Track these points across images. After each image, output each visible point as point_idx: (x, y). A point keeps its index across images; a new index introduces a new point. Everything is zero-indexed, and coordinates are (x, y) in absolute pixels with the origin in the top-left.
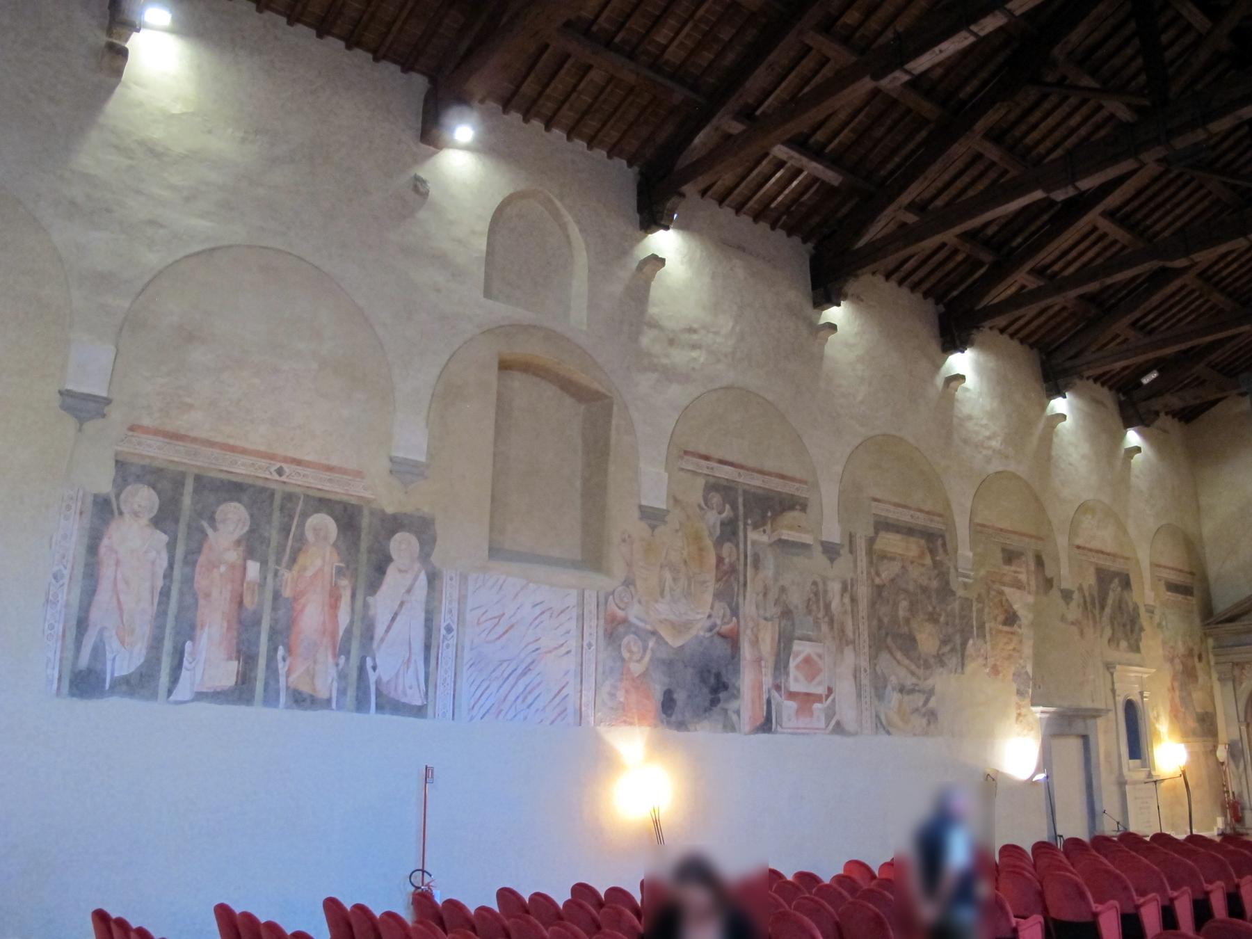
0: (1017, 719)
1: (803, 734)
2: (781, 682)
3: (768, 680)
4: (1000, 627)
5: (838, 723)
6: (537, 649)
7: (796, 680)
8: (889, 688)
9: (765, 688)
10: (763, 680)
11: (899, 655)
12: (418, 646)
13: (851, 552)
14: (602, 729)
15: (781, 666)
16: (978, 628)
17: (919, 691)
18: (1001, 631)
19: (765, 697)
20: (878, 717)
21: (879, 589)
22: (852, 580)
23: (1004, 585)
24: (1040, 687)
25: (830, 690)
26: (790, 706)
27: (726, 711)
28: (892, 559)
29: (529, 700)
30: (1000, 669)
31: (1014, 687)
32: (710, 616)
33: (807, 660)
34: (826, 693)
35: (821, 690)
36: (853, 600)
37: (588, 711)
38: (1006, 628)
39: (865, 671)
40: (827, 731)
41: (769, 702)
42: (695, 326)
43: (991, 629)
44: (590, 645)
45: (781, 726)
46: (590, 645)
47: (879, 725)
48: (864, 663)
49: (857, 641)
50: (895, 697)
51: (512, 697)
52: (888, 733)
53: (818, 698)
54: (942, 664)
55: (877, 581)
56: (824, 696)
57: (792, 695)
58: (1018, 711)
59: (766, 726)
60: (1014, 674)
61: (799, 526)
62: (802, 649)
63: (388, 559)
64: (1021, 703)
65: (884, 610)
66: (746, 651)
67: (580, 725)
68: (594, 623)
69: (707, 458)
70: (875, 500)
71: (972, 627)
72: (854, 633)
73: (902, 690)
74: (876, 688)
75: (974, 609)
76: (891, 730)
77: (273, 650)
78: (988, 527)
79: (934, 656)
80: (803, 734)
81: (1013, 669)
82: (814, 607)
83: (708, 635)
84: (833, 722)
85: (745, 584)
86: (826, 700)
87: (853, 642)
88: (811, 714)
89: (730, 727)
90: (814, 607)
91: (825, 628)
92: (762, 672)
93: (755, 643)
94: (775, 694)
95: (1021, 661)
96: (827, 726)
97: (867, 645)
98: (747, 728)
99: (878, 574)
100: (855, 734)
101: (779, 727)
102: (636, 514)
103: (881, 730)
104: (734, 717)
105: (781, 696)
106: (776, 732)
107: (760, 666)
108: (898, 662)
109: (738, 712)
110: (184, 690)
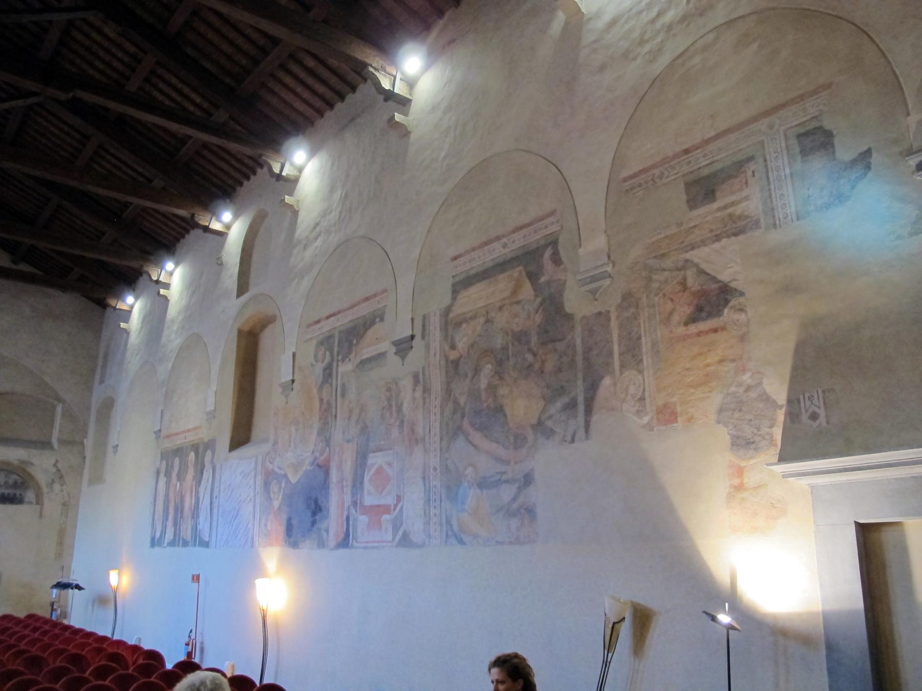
0: (730, 497)
1: (373, 548)
2: (357, 498)
3: (348, 499)
4: (681, 330)
5: (405, 535)
6: (240, 501)
7: (370, 494)
8: (466, 484)
9: (346, 505)
10: (345, 497)
11: (477, 437)
12: (209, 509)
13: (423, 337)
14: (260, 549)
15: (358, 484)
16: (621, 354)
17: (506, 481)
18: (685, 338)
19: (345, 514)
20: (448, 522)
21: (455, 365)
22: (424, 369)
23: (693, 249)
24: (814, 417)
25: (399, 498)
26: (363, 519)
27: (319, 529)
28: (474, 317)
29: (236, 534)
30: (679, 409)
31: (723, 435)
32: (313, 452)
33: (379, 471)
34: (395, 502)
35: (389, 500)
36: (426, 390)
37: (256, 538)
38: (693, 329)
39: (435, 469)
40: (394, 544)
41: (348, 519)
42: (318, 220)
43: (654, 344)
44: (258, 493)
45: (357, 542)
46: (258, 493)
47: (450, 533)
48: (434, 461)
49: (427, 437)
50: (472, 495)
51: (232, 533)
52: (461, 542)
53: (386, 509)
54: (549, 433)
55: (453, 355)
56: (392, 506)
57: (367, 510)
58: (736, 482)
59: (345, 542)
60: (720, 411)
61: (377, 339)
62: (376, 460)
63: (204, 466)
64: (743, 464)
65: (461, 389)
66: (334, 475)
67: (252, 547)
68: (260, 477)
69: (318, 322)
70: (455, 258)
71: (611, 353)
72: (424, 428)
73: (483, 484)
74: (448, 488)
75: (614, 324)
76: (464, 537)
77: (180, 521)
78: (654, 166)
79: (533, 426)
80: (373, 548)
81: (717, 399)
82: (388, 415)
83: (313, 467)
84: (400, 533)
85: (336, 416)
86: (394, 510)
87: (423, 439)
88: (379, 526)
89: (322, 544)
90: (388, 415)
91: (395, 432)
92: (343, 491)
93: (340, 468)
94: (353, 511)
95: (746, 378)
96: (394, 539)
97: (437, 439)
98: (332, 543)
99: (453, 347)
100: (421, 546)
101: (354, 542)
102: (280, 390)
103: (452, 540)
104: (325, 534)
105: (356, 511)
106: (352, 547)
107: (342, 487)
108: (475, 446)
109: (327, 531)
110: (165, 544)
